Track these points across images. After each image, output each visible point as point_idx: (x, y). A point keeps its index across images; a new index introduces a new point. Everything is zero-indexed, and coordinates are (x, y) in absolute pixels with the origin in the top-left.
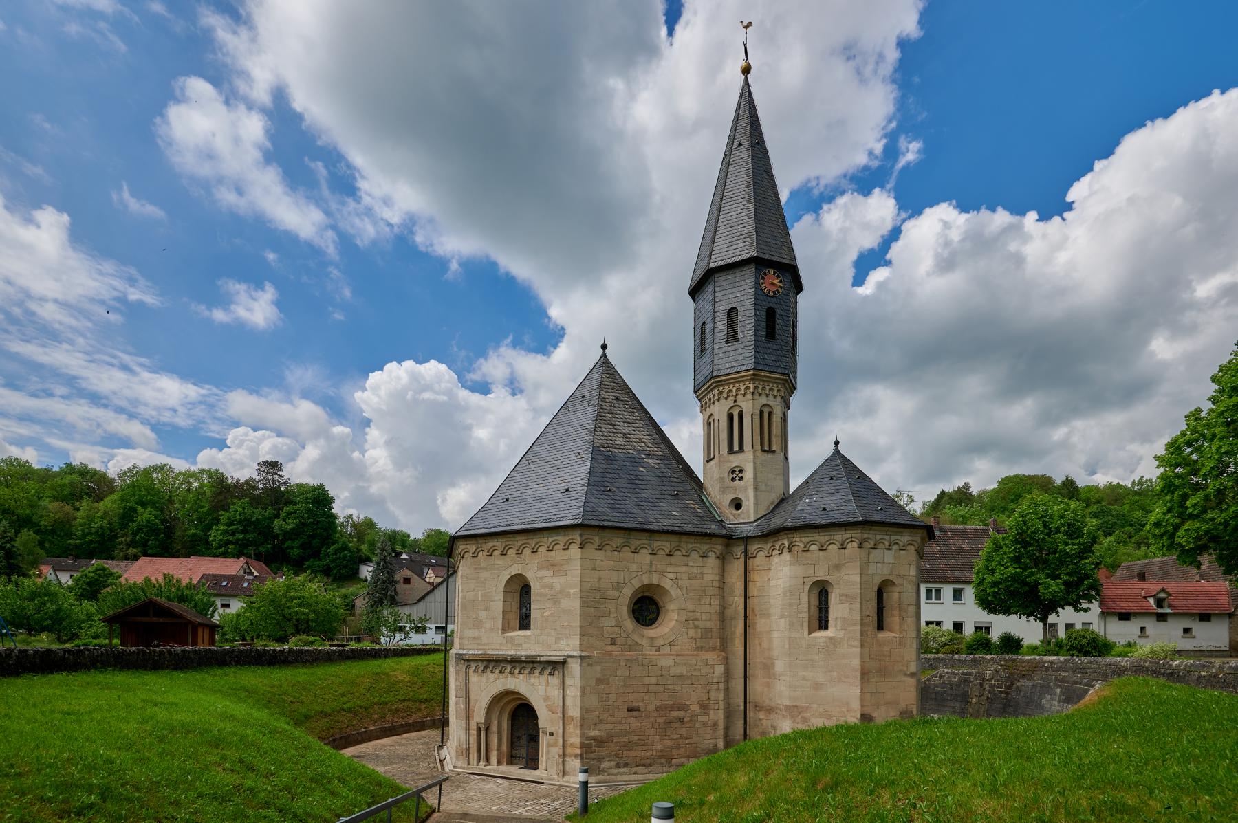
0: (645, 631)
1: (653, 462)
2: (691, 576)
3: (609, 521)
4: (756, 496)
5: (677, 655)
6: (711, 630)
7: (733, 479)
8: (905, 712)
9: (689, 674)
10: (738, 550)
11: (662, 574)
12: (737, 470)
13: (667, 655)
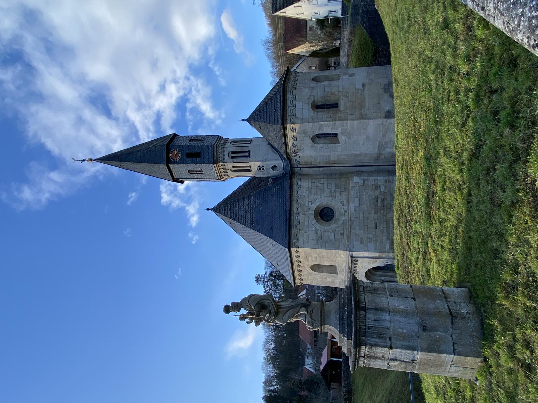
0: (337, 217)
1: (257, 202)
3: (286, 235)
4: (271, 160)
5: (349, 202)
6: (336, 183)
7: (263, 169)
8: (385, 89)
9: (359, 196)
10: (296, 170)
11: (309, 209)
12: (259, 168)
13: (349, 206)
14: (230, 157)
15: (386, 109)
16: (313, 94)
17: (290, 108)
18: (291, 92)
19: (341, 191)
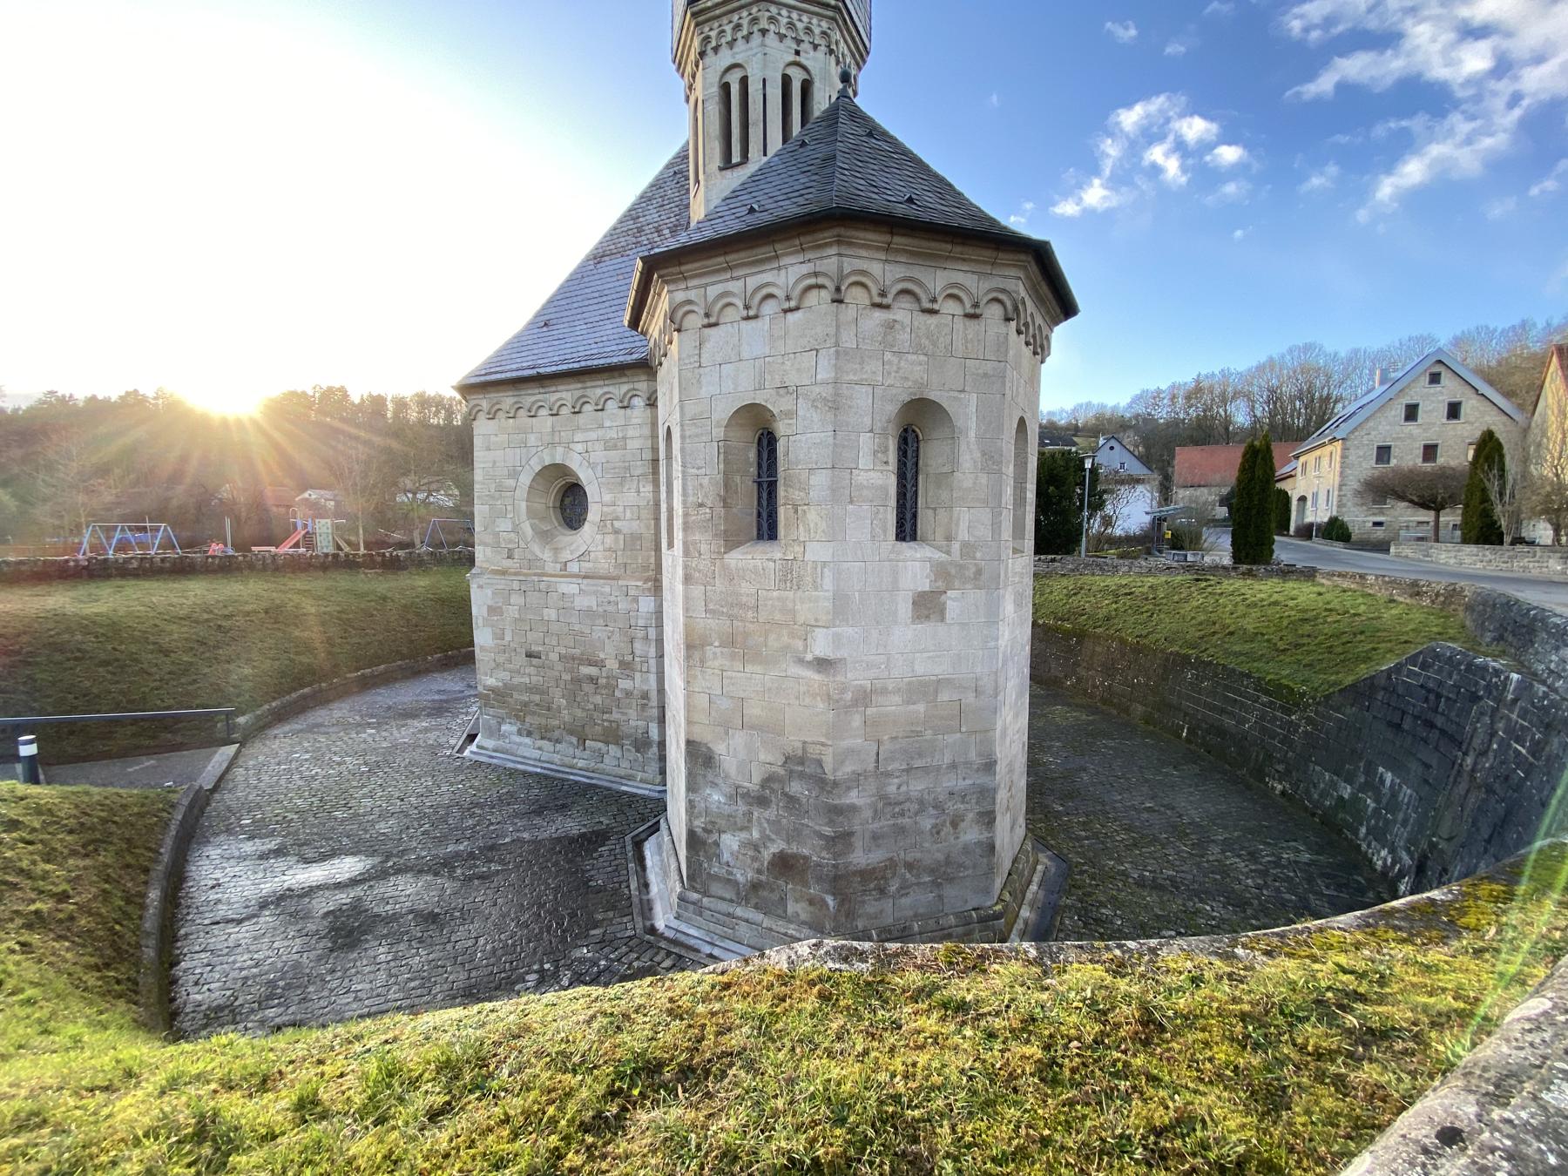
2: (610, 445)
5: (585, 577)
6: (640, 537)
9: (600, 609)
14: (728, 78)
15: (719, 748)
16: (803, 408)
17: (735, 286)
18: (816, 274)
19: (619, 553)
